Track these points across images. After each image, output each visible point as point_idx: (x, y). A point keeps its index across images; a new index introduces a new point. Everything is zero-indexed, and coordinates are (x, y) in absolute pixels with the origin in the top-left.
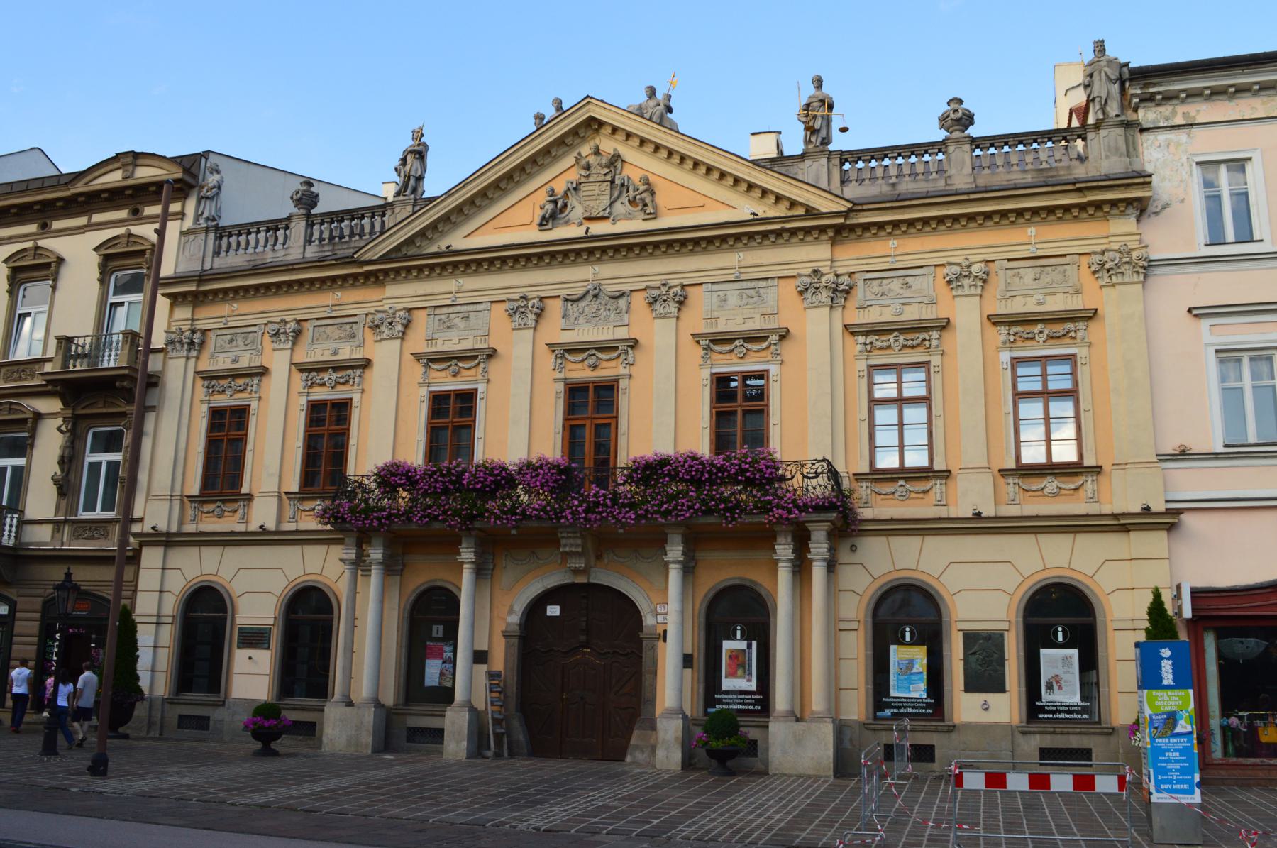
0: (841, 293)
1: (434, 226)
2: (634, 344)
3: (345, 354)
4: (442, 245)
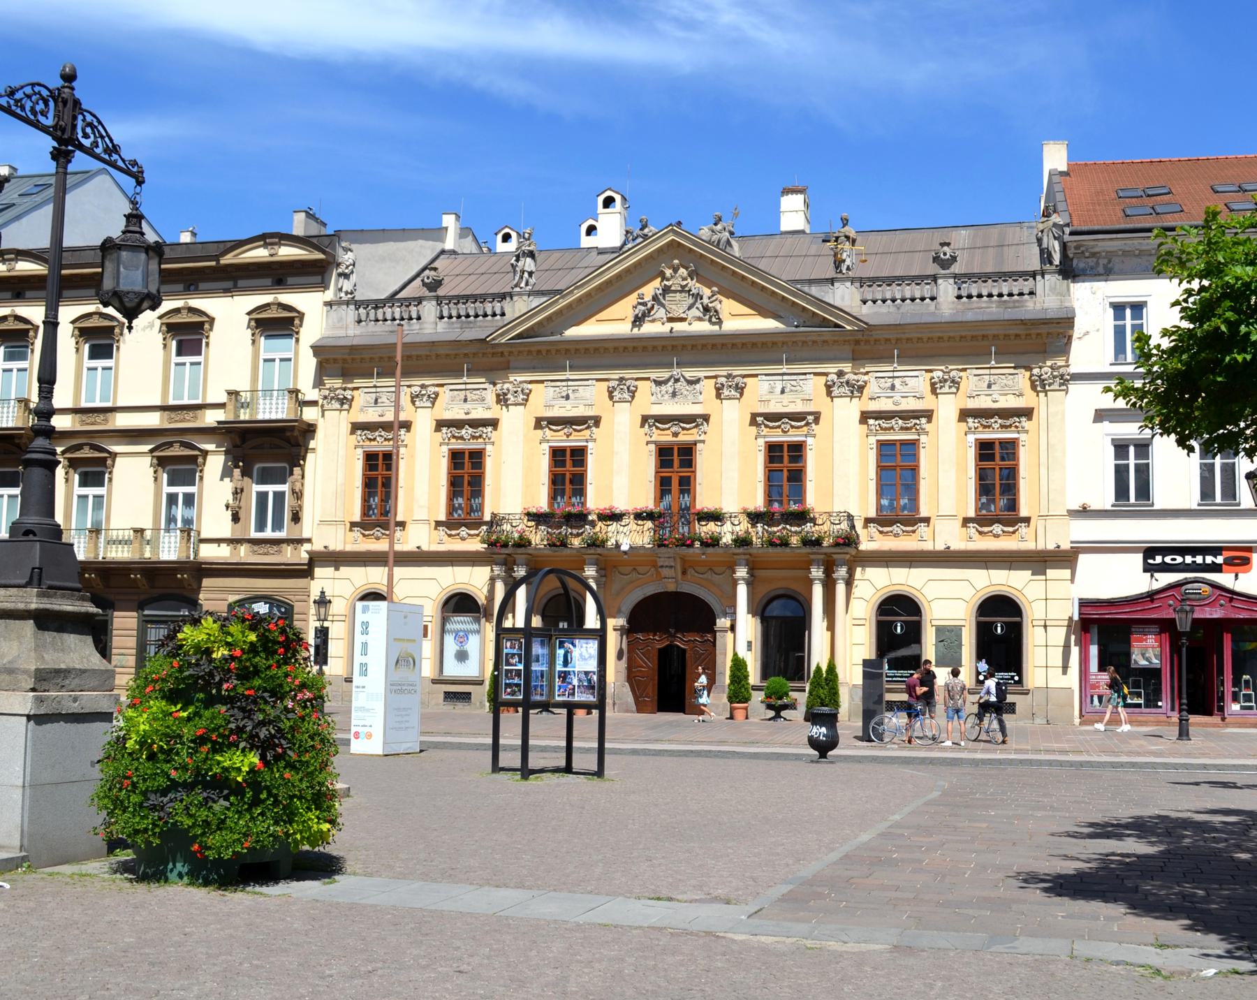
0: (857, 390)
2: (706, 418)
3: (479, 413)
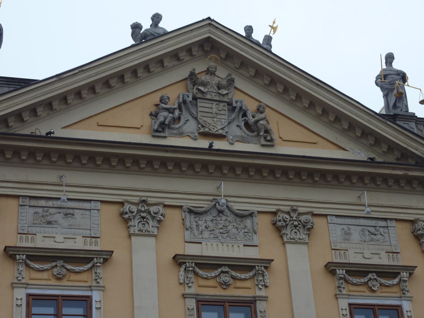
1: (33, 110)
4: (42, 129)
